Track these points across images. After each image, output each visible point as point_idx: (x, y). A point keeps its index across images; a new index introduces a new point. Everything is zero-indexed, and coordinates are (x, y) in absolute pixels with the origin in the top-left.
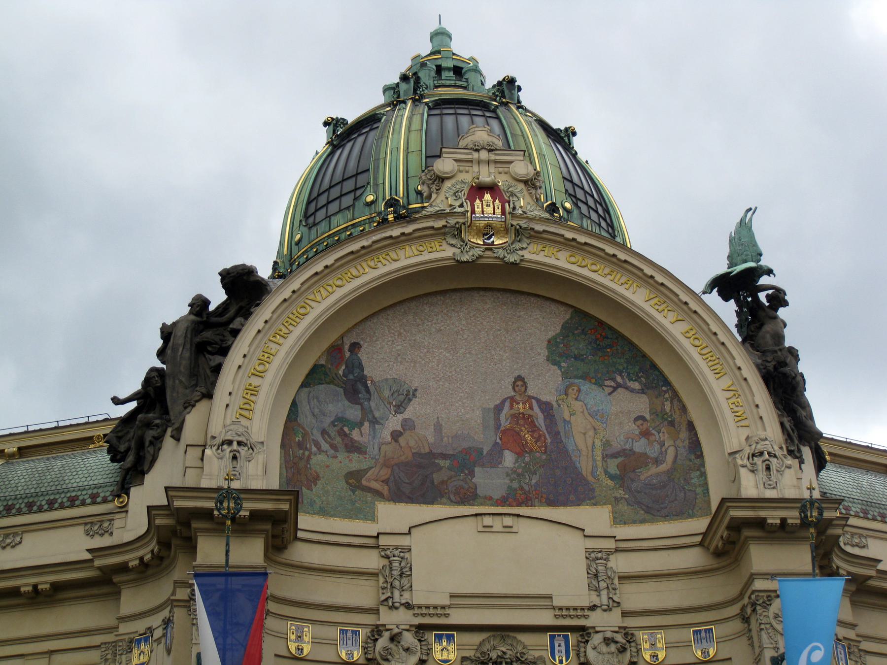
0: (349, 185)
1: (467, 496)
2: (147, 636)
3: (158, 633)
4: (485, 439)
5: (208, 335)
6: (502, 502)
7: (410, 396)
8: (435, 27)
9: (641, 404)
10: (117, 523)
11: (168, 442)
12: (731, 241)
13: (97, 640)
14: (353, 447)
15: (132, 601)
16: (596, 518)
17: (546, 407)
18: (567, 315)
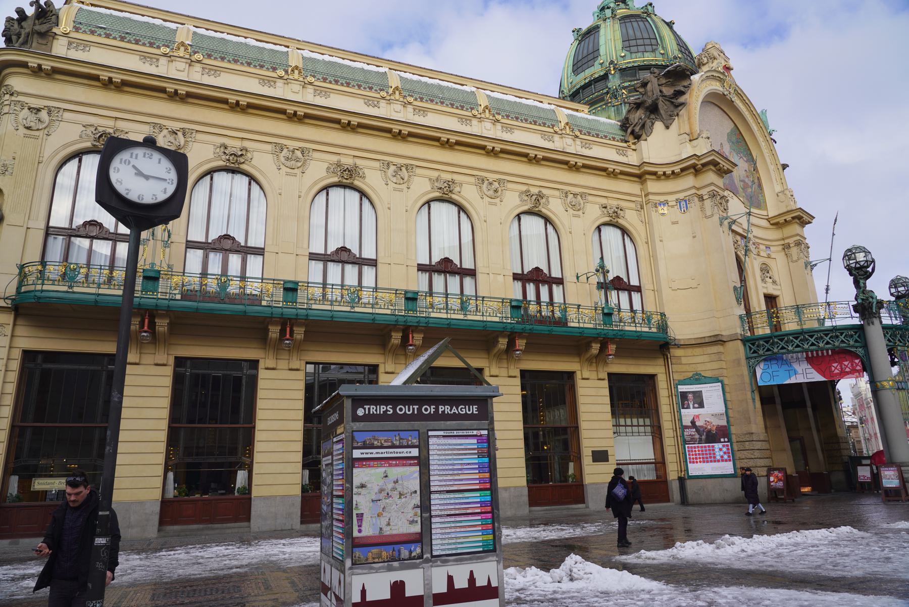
3: (670, 204)
13: (633, 199)
15: (653, 186)
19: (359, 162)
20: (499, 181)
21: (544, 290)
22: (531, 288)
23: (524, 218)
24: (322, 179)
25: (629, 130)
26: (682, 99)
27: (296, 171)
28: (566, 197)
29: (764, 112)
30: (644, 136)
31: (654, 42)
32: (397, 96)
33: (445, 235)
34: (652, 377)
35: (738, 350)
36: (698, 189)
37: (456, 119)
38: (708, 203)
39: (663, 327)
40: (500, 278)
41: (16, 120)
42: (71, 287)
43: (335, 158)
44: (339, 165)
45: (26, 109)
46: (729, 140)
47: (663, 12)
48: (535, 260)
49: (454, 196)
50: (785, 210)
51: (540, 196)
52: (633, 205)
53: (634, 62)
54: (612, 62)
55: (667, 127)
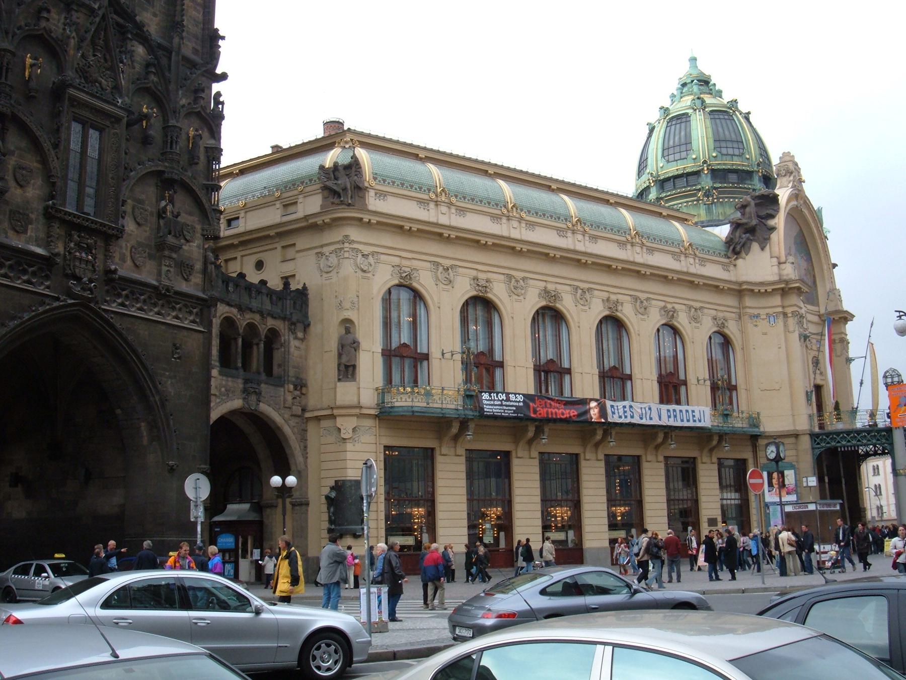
0: (735, 145)
2: (758, 316)
13: (735, 310)
15: (748, 301)
20: (648, 299)
25: (731, 248)
26: (771, 222)
27: (521, 298)
28: (690, 310)
29: (820, 210)
30: (743, 254)
31: (741, 146)
35: (806, 441)
36: (783, 307)
37: (615, 245)
39: (754, 421)
42: (428, 404)
44: (546, 291)
45: (360, 256)
46: (795, 243)
47: (743, 107)
53: (724, 164)
54: (705, 162)
55: (762, 249)
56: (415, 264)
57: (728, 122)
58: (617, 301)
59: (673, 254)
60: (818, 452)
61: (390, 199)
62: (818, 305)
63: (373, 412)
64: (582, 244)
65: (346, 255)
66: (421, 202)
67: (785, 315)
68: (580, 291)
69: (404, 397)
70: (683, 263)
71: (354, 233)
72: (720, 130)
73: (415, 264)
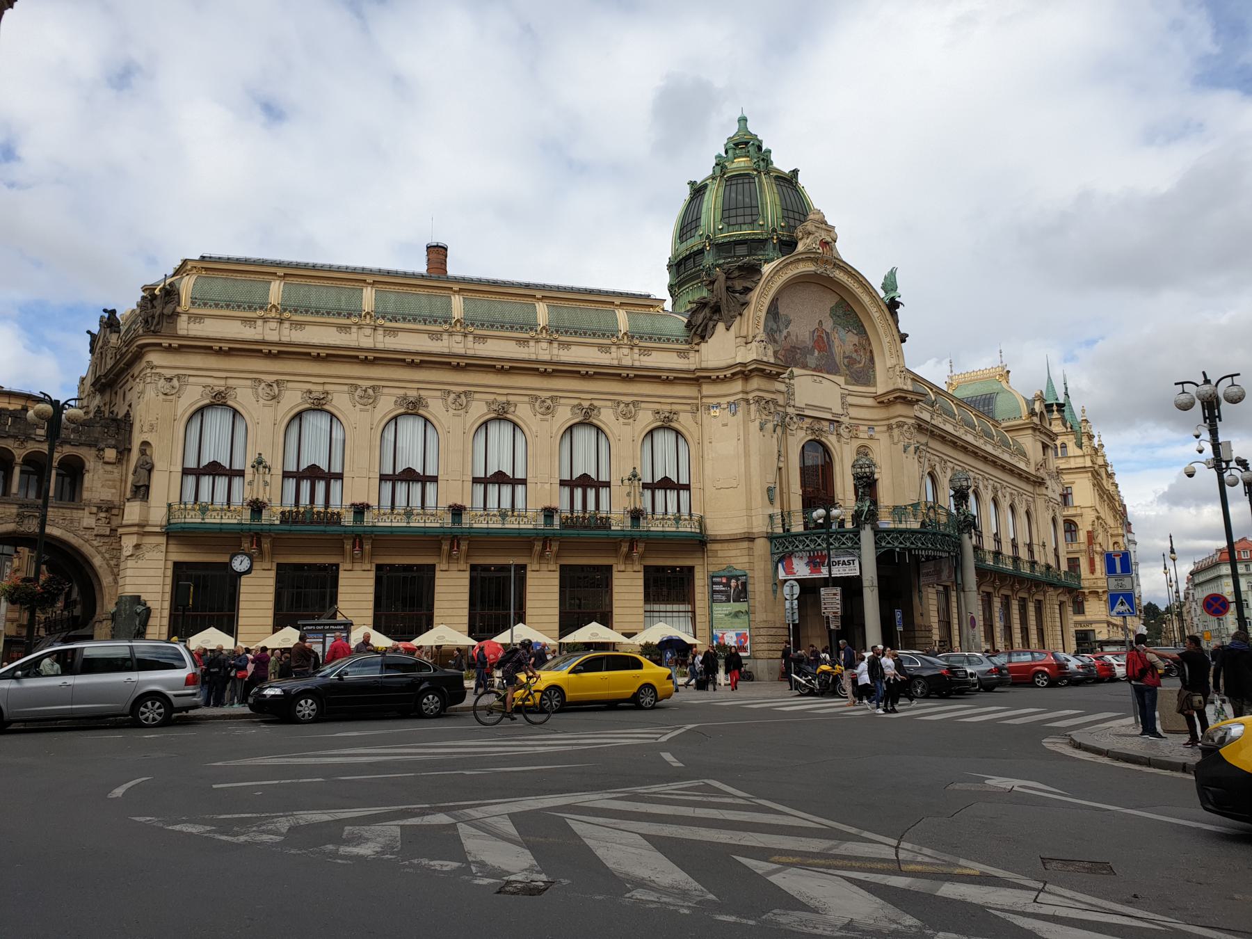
0: (748, 211)
1: (805, 367)
4: (809, 343)
5: (729, 283)
6: (814, 370)
7: (789, 322)
8: (739, 115)
9: (855, 339)
10: (692, 354)
11: (721, 326)
12: (886, 278)
14: (775, 341)
15: (707, 389)
16: (841, 380)
17: (827, 334)
18: (837, 299)
19: (422, 393)
20: (552, 398)
21: (591, 494)
22: (578, 493)
23: (575, 431)
24: (391, 411)
32: (458, 328)
33: (500, 451)
34: (691, 569)
38: (753, 408)
40: (547, 486)
41: (156, 388)
43: (402, 392)
44: (405, 398)
48: (584, 465)
49: (509, 416)
50: (891, 388)
51: (592, 408)
52: (688, 408)
56: (231, 382)
57: (747, 186)
58: (508, 403)
59: (601, 347)
60: (776, 557)
61: (207, 321)
62: (875, 385)
63: (158, 529)
64: (461, 345)
65: (148, 380)
66: (245, 320)
67: (747, 401)
68: (452, 396)
69: (192, 513)
70: (614, 355)
71: (154, 358)
72: (733, 195)
73: (231, 382)
